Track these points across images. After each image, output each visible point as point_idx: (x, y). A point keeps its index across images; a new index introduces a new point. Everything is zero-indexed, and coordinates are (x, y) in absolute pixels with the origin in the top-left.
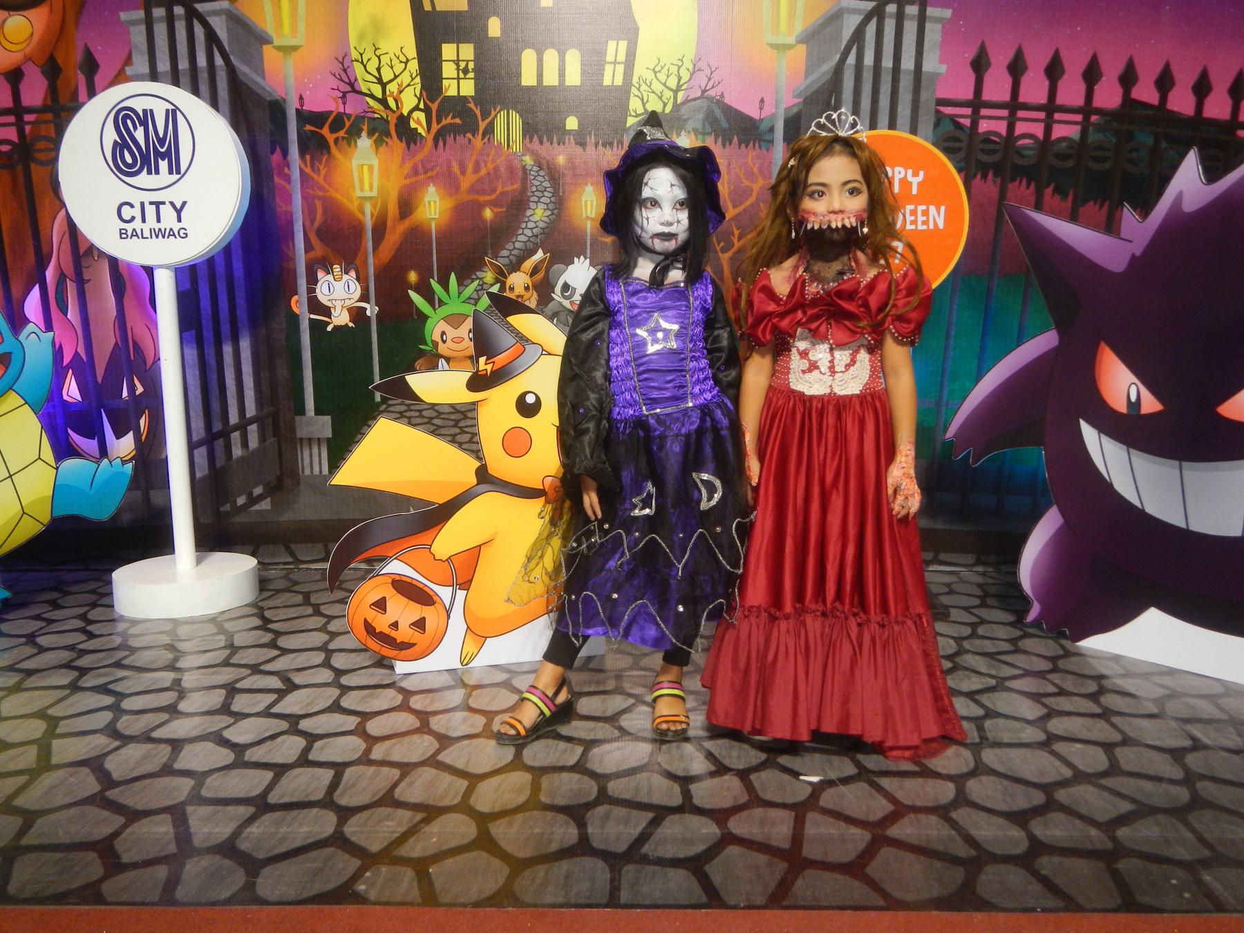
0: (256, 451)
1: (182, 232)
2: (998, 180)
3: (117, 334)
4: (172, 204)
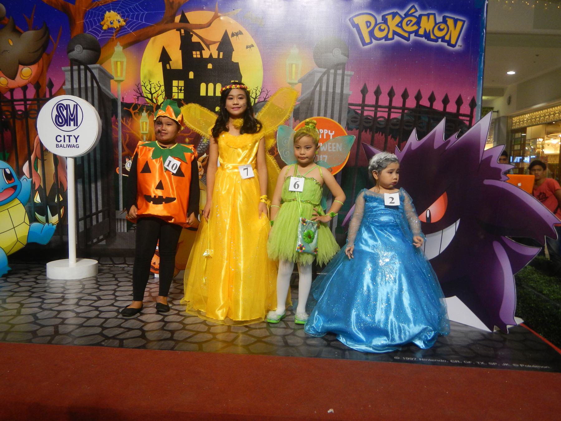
0: (101, 222)
1: (77, 146)
2: (371, 134)
3: (55, 179)
4: (74, 136)
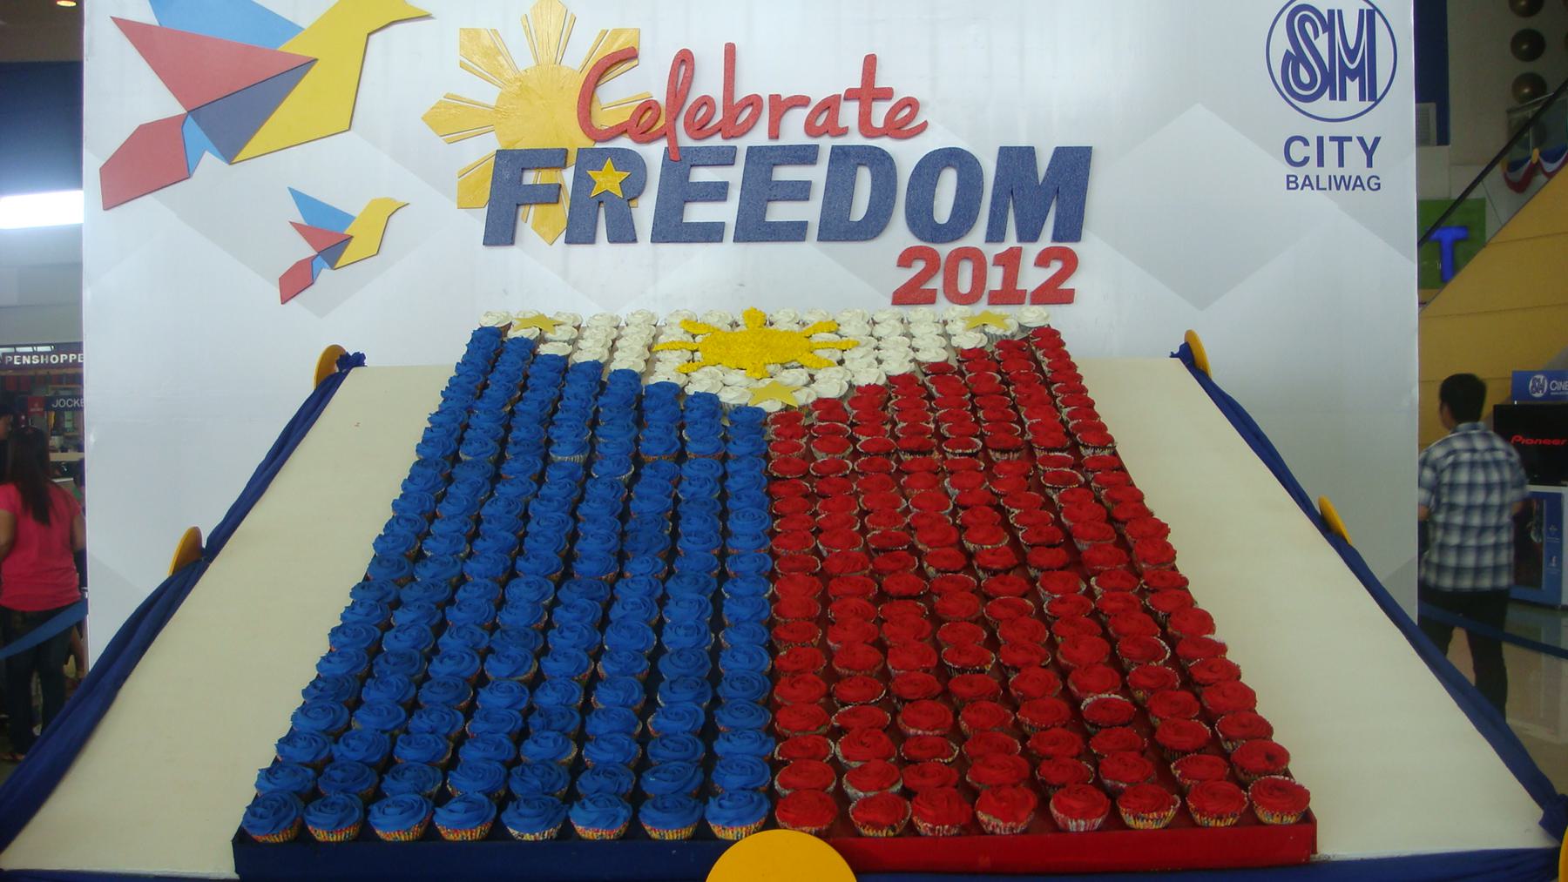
1: (1373, 181)
4: (1361, 140)
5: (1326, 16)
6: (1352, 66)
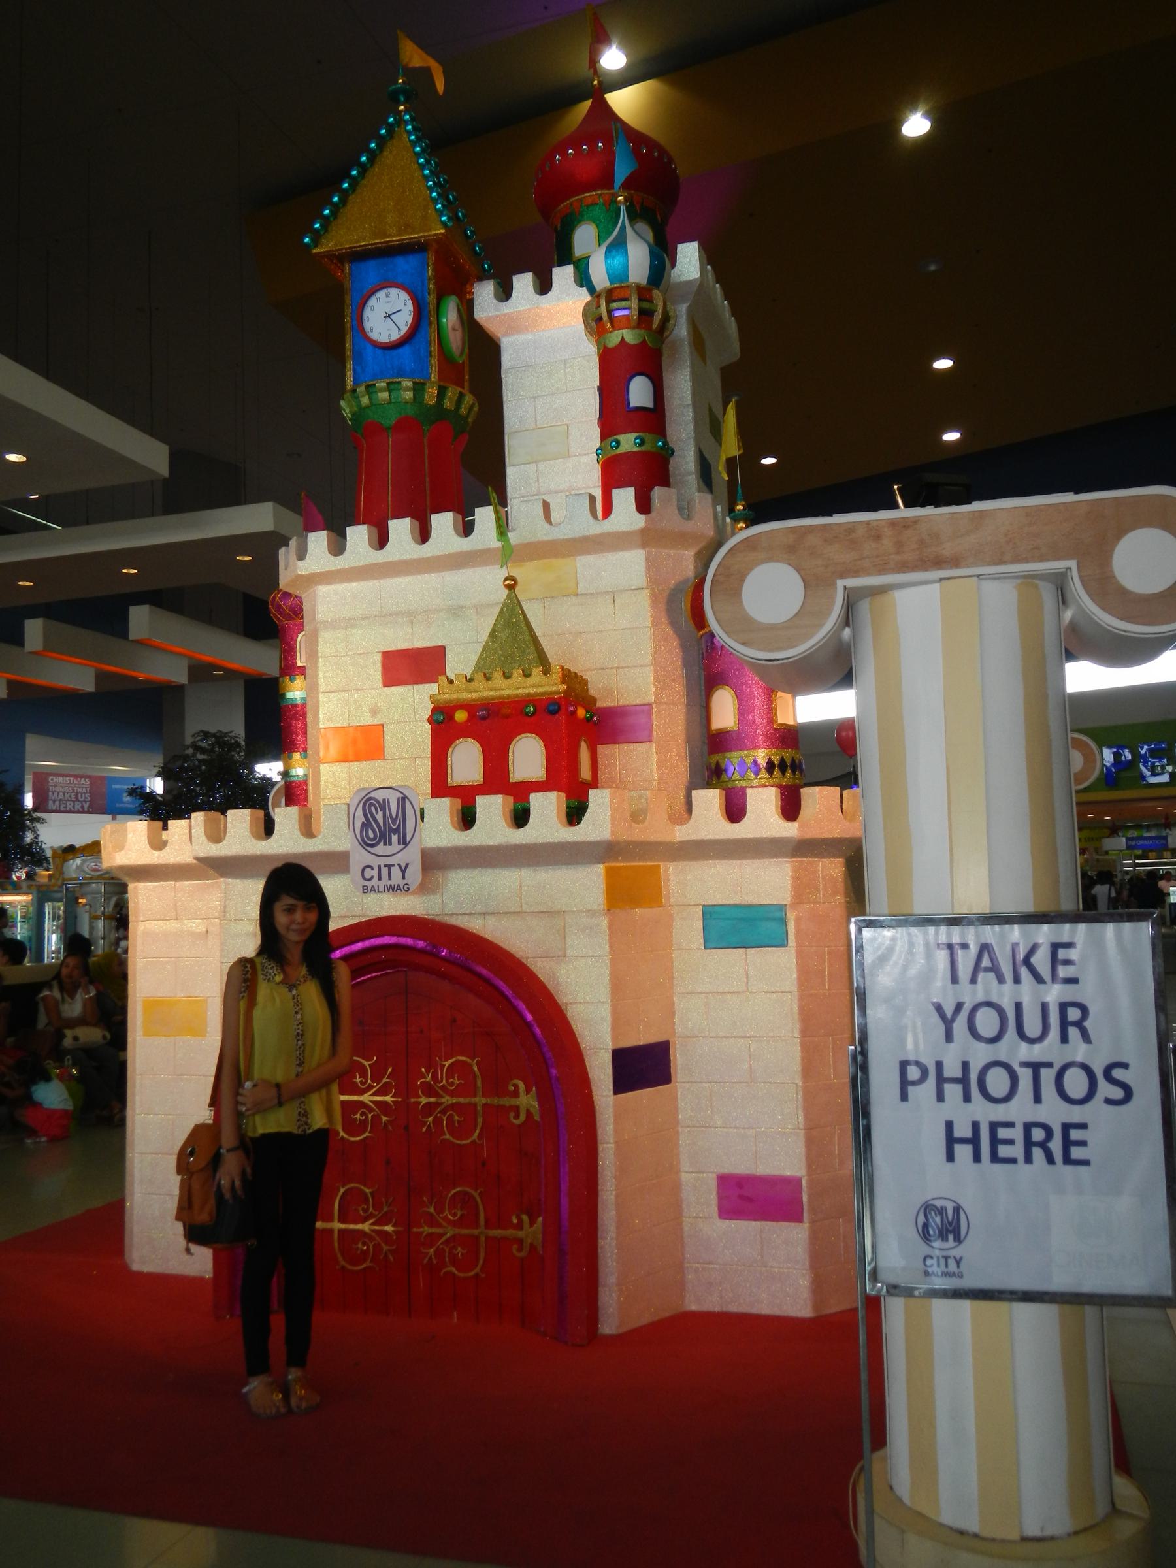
1: (406, 886)
4: (399, 865)
5: (382, 802)
6: (394, 827)
